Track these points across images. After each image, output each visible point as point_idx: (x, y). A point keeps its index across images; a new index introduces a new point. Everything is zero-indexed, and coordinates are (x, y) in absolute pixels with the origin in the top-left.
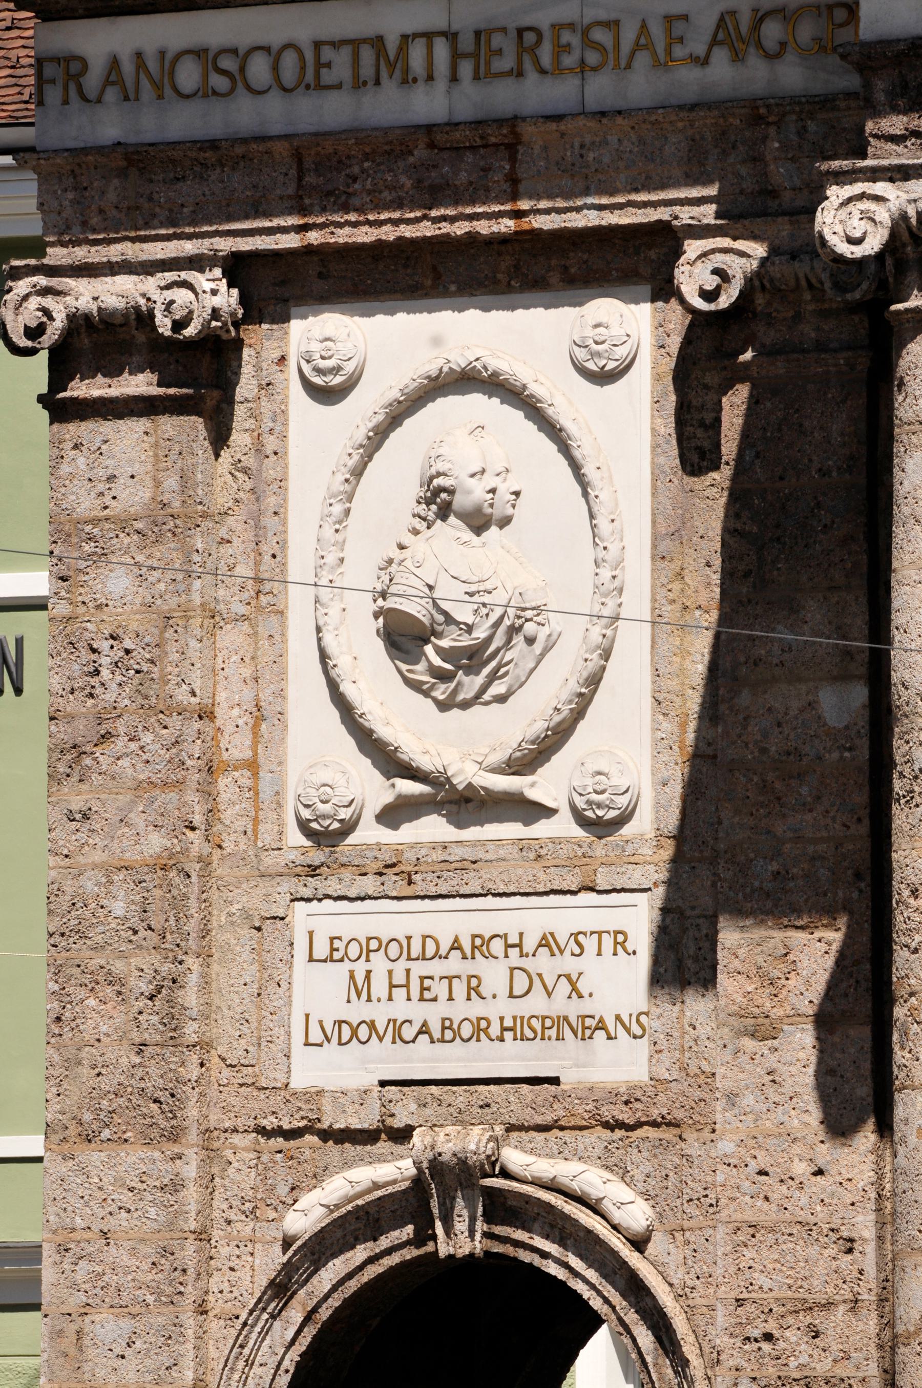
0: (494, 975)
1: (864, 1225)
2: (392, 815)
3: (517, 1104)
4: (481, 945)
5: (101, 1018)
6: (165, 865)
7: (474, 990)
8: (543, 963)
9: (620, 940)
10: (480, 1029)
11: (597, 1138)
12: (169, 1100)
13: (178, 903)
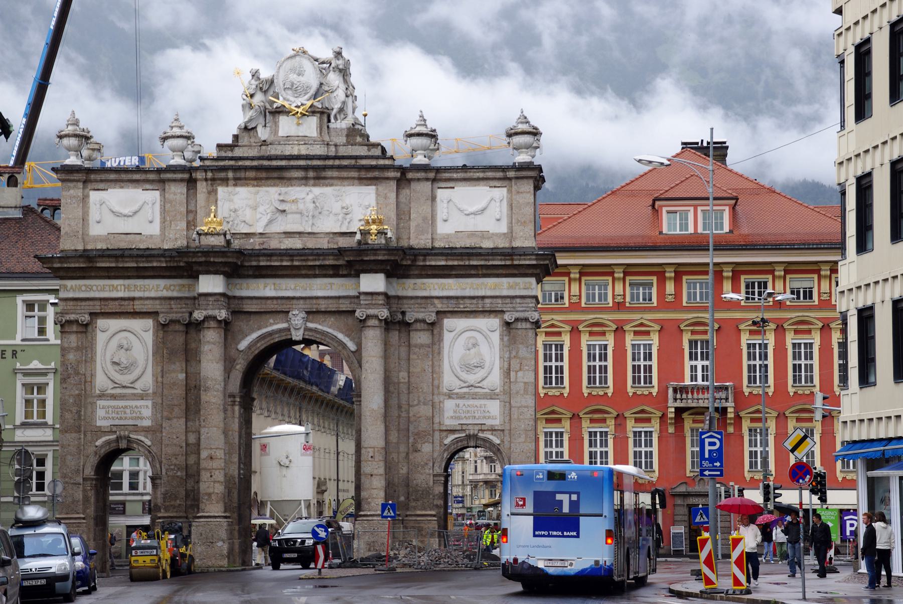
0: (128, 411)
1: (184, 445)
3: (131, 428)
4: (126, 407)
5: (68, 416)
6: (79, 395)
7: (125, 413)
8: (136, 410)
9: (147, 407)
10: (126, 418)
11: (143, 433)
12: (79, 427)
13: (81, 401)
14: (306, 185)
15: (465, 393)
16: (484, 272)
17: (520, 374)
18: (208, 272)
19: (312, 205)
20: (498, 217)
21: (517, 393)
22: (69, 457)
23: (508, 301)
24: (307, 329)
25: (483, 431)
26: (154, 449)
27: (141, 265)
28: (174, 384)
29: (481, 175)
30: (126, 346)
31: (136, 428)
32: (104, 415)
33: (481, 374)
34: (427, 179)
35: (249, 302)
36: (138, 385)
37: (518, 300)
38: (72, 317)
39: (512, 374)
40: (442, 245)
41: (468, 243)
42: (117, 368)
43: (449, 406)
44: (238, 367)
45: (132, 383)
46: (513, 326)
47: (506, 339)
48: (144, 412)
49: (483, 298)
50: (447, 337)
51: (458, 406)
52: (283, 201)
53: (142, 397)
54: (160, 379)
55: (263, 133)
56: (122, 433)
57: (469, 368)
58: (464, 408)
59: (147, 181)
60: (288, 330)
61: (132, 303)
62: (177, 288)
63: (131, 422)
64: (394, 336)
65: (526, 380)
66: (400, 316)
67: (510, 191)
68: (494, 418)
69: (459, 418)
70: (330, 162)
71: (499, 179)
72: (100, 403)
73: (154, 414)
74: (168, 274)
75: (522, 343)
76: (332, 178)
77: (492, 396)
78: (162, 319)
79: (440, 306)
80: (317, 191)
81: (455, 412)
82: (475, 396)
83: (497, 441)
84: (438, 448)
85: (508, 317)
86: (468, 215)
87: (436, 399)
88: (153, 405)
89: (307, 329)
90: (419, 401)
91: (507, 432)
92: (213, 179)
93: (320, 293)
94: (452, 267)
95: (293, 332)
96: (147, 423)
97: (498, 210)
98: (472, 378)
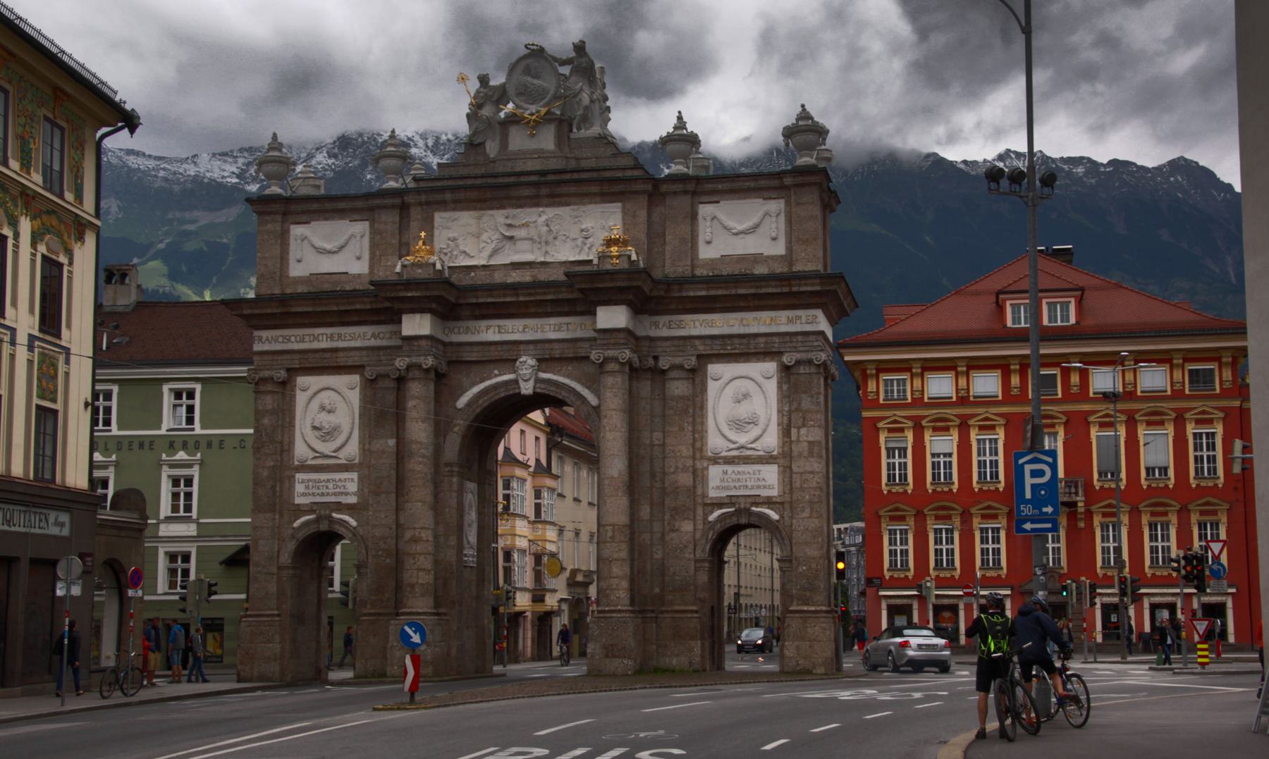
0: (331, 485)
2: (315, 458)
14: (537, 205)
15: (734, 457)
16: (756, 303)
17: (803, 431)
18: (413, 311)
19: (545, 228)
20: (774, 235)
21: (800, 455)
22: (261, 542)
23: (787, 338)
24: (538, 381)
25: (757, 504)
26: (361, 531)
27: (342, 308)
28: (383, 452)
29: (752, 184)
30: (328, 407)
31: (339, 507)
32: (303, 490)
33: (756, 432)
34: (685, 192)
35: (468, 348)
37: (800, 338)
38: (266, 374)
39: (794, 431)
40: (705, 273)
41: (737, 269)
42: (317, 433)
43: (715, 472)
44: (456, 429)
45: (335, 451)
46: (794, 371)
47: (785, 387)
48: (349, 486)
49: (756, 335)
50: (712, 387)
51: (725, 473)
52: (510, 226)
54: (367, 446)
55: (492, 148)
56: (323, 512)
57: (739, 424)
58: (734, 476)
60: (516, 382)
62: (388, 335)
63: (333, 499)
64: (645, 388)
65: (810, 439)
66: (651, 362)
67: (788, 204)
68: (770, 487)
69: (727, 488)
70: (568, 176)
71: (775, 189)
72: (299, 476)
73: (360, 489)
74: (375, 318)
75: (805, 392)
76: (568, 195)
77: (767, 459)
78: (368, 373)
79: (701, 348)
80: (550, 212)
81: (722, 480)
82: (747, 460)
83: (775, 516)
84: (700, 527)
85: (786, 359)
86: (736, 234)
87: (699, 465)
88: (359, 478)
89: (538, 381)
90: (677, 468)
91: (787, 506)
93: (553, 336)
94: (714, 299)
96: (353, 500)
97: (774, 226)
98: (743, 439)
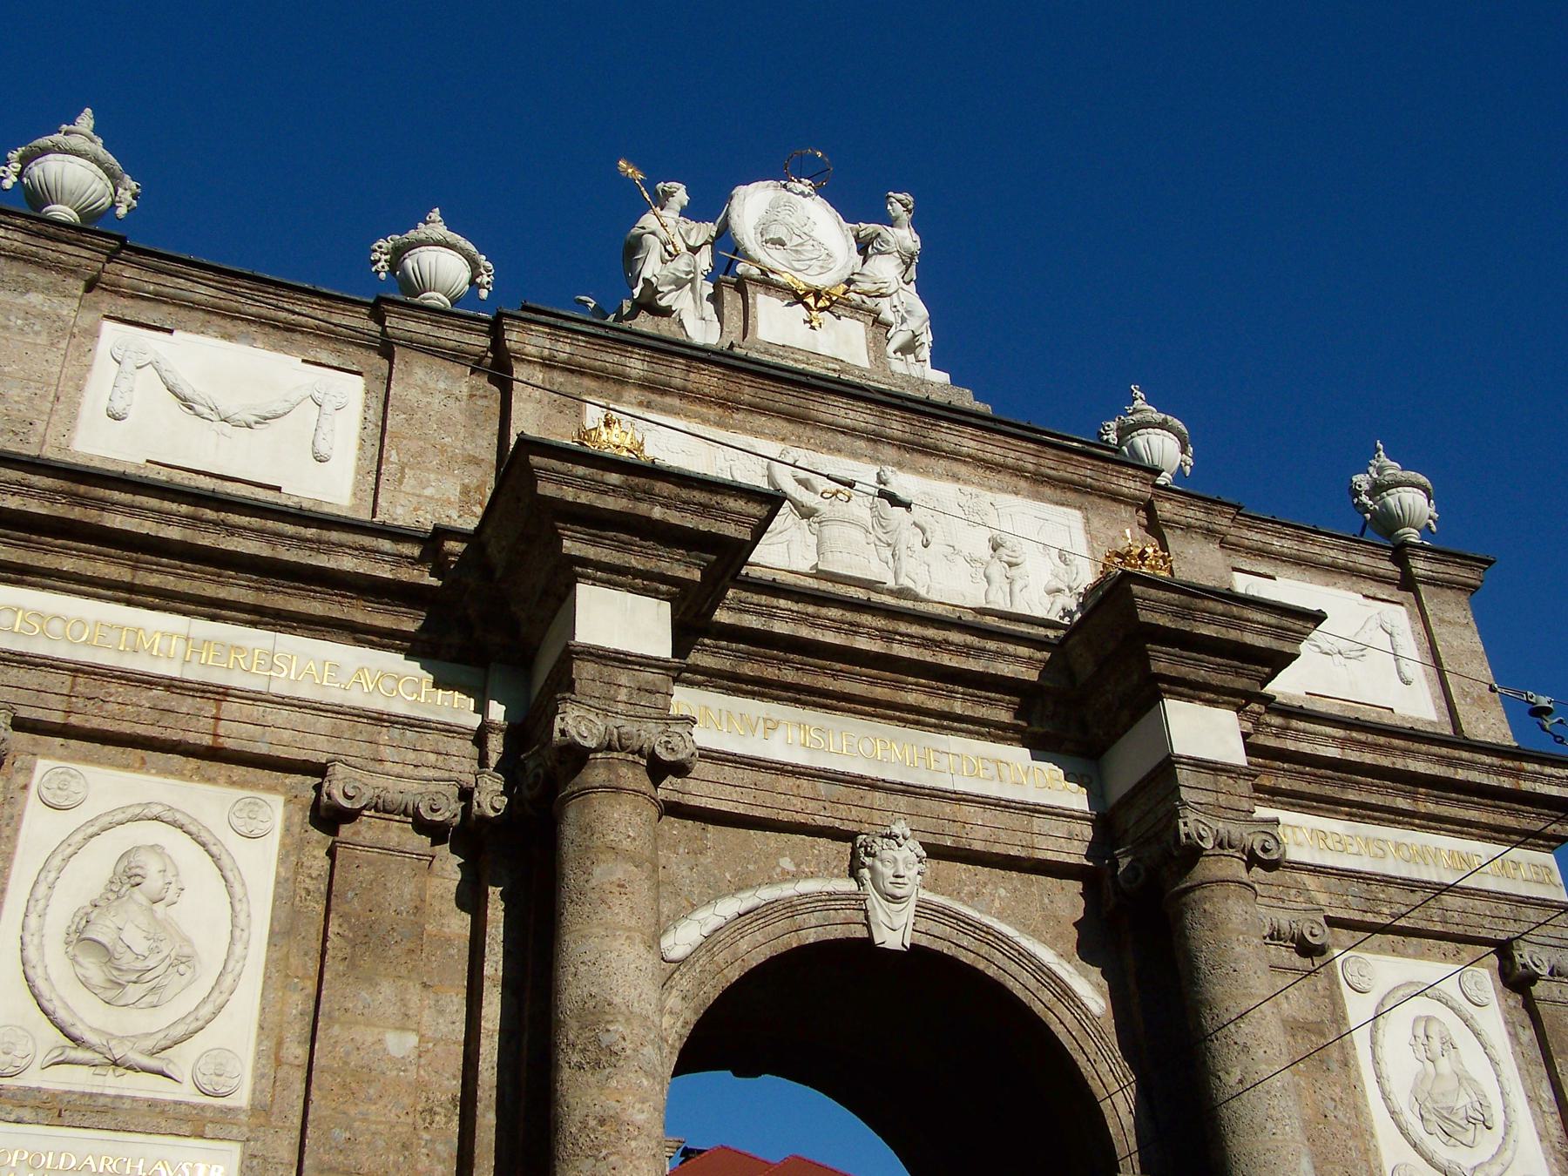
36: (183, 1060)
53: (194, 1122)
59: (328, 335)
61: (210, 708)
76: (954, 456)
92: (574, 369)
95: (880, 911)
